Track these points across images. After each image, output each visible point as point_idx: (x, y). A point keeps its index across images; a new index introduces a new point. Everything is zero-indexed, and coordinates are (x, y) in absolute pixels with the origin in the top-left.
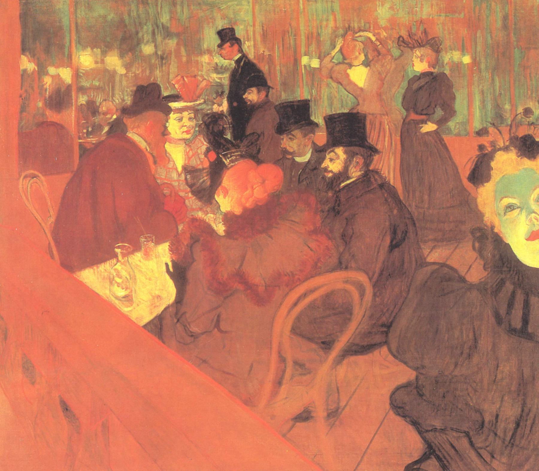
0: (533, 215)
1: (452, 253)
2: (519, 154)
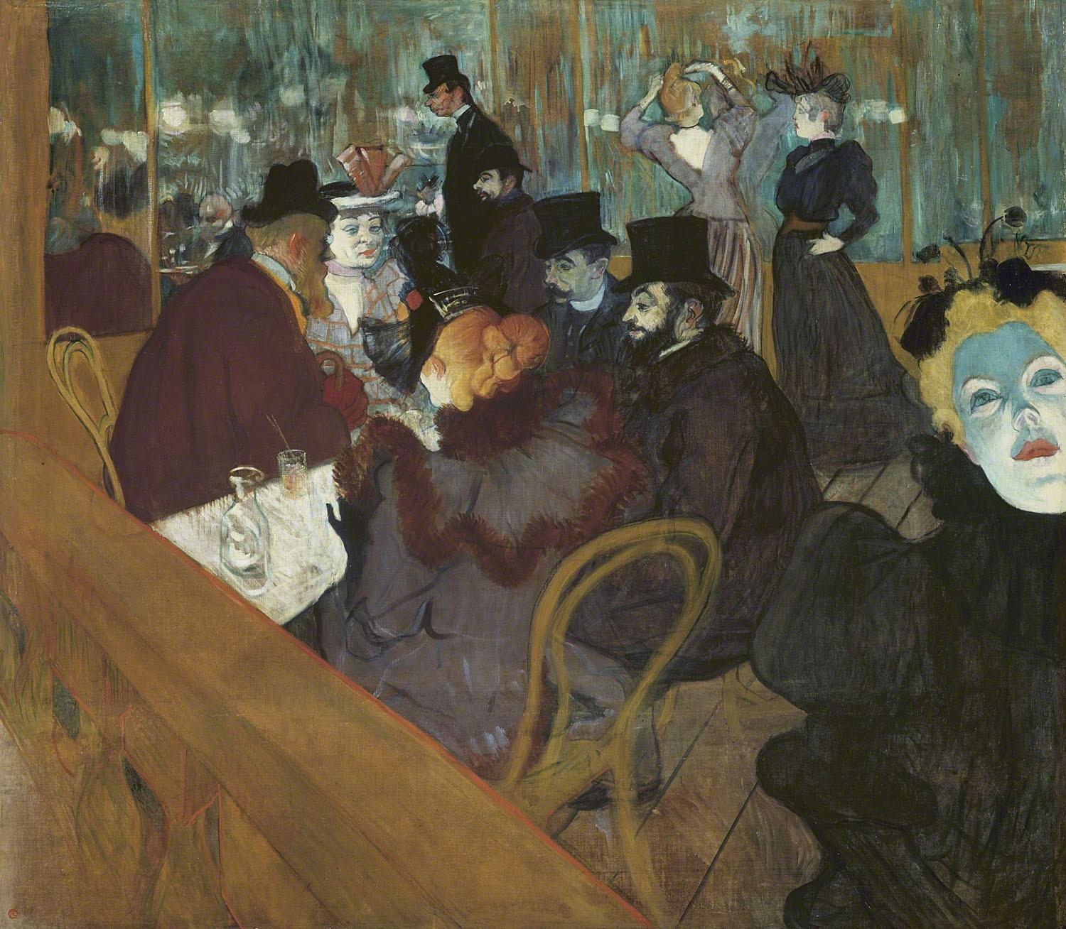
0: (1027, 411)
1: (873, 483)
2: (999, 295)
